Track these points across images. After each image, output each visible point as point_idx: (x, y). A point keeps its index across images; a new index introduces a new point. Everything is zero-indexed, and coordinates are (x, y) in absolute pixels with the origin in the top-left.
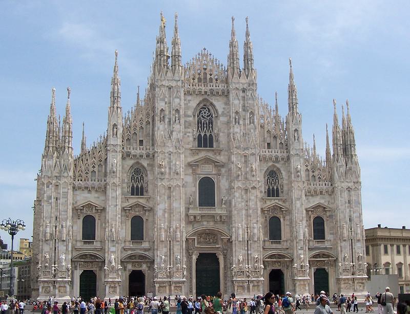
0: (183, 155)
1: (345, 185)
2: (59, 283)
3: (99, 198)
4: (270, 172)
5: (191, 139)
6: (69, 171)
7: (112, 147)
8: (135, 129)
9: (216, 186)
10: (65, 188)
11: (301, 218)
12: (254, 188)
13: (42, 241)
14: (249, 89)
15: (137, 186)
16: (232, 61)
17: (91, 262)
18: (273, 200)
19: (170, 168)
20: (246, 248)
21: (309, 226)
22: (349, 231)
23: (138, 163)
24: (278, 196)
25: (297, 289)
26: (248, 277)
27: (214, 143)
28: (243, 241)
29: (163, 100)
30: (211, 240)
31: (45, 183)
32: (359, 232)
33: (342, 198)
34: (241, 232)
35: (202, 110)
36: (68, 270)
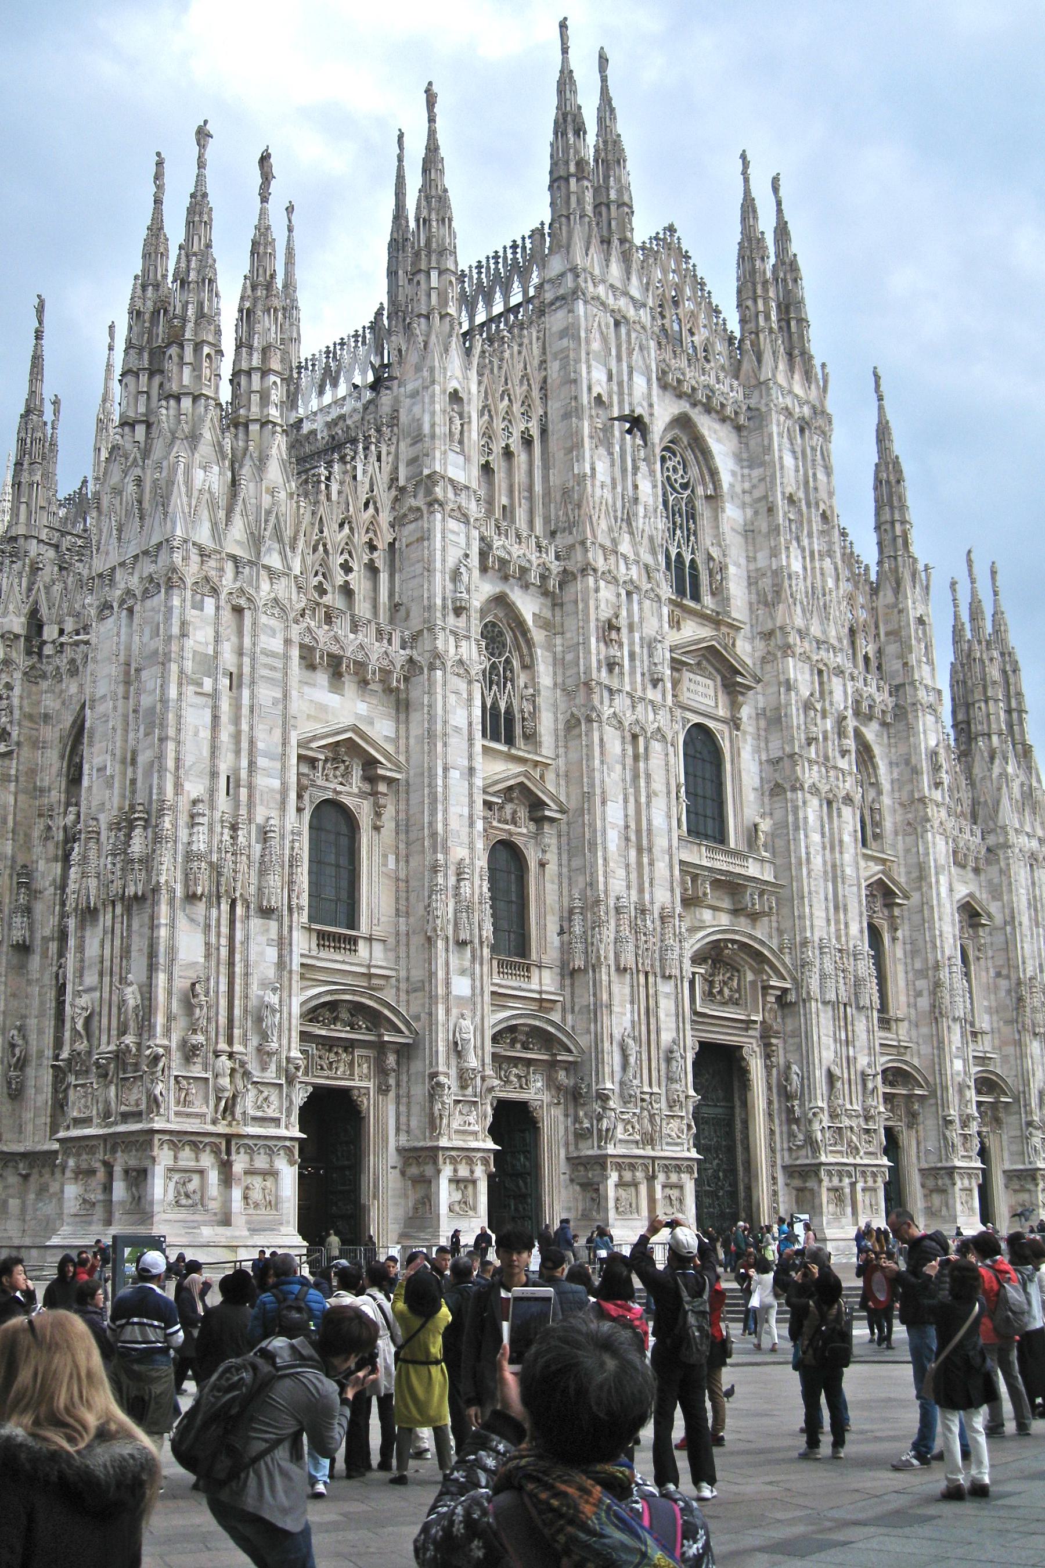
1: (1023, 840)
2: (250, 1151)
3: (372, 723)
6: (293, 549)
7: (451, 495)
9: (728, 766)
10: (273, 634)
12: (848, 800)
13: (171, 902)
14: (813, 423)
16: (761, 308)
17: (349, 1046)
19: (632, 656)
26: (854, 1150)
27: (707, 600)
30: (726, 991)
31: (189, 581)
36: (290, 1081)
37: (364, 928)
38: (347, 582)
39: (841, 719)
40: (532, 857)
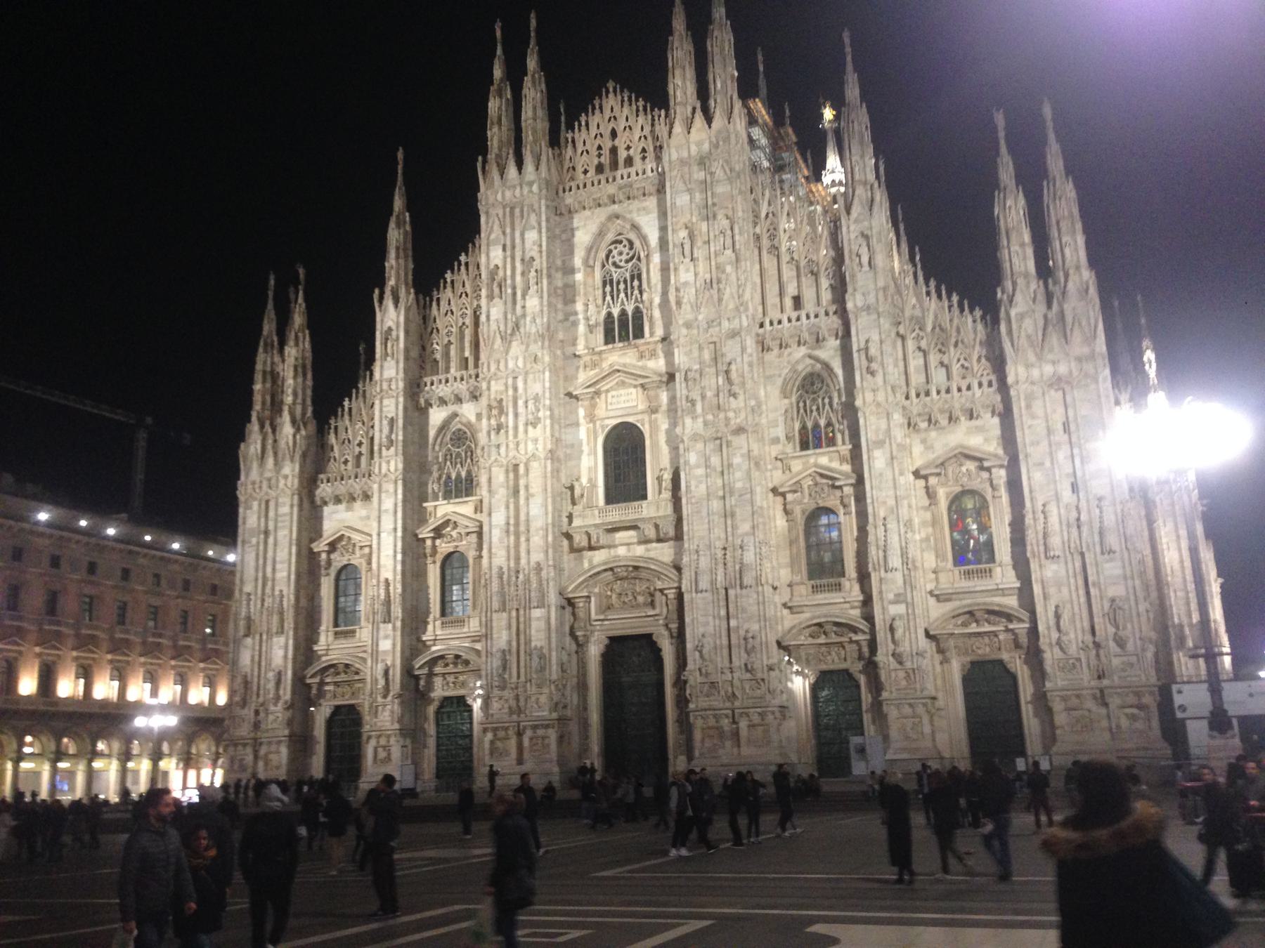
0: (547, 374)
4: (804, 379)
5: (582, 328)
8: (449, 334)
9: (648, 443)
10: (284, 504)
11: (891, 502)
12: (740, 430)
15: (459, 475)
18: (812, 460)
20: (723, 612)
21: (935, 522)
22: (1068, 525)
23: (455, 415)
24: (832, 442)
25: (894, 733)
28: (714, 590)
29: (496, 242)
30: (641, 599)
32: (1110, 519)
33: (1033, 417)
34: (704, 562)
35: (612, 247)
37: (363, 623)
38: (360, 454)
39: (727, 372)
40: (471, 555)
